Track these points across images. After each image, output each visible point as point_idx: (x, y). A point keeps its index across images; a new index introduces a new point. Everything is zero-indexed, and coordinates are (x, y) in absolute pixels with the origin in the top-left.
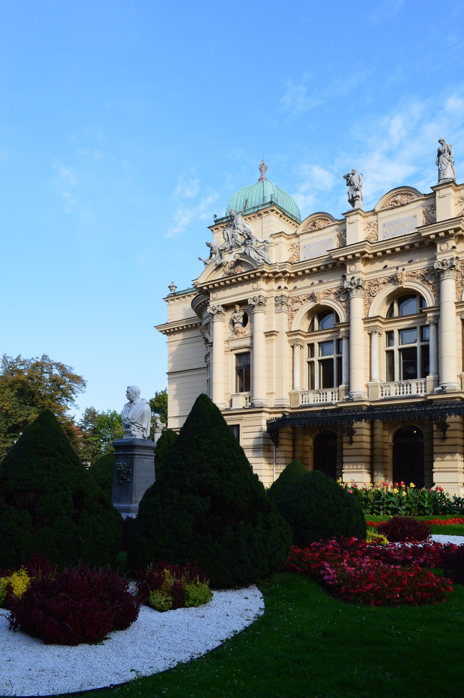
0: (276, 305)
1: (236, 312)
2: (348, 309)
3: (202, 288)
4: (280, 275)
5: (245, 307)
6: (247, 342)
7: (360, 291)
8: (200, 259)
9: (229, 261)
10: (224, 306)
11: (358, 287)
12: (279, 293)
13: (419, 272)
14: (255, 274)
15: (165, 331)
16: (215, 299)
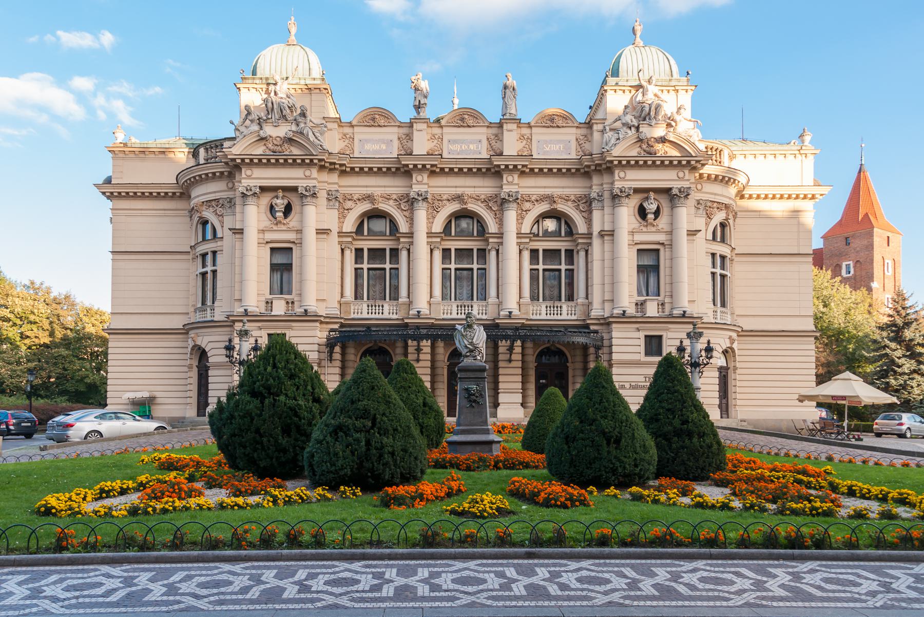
0: (329, 200)
1: (277, 197)
2: (411, 220)
3: (234, 160)
4: (337, 166)
5: (287, 194)
6: (291, 236)
7: (425, 204)
8: (232, 123)
9: (274, 135)
10: (260, 187)
11: (425, 199)
12: (335, 187)
13: (483, 197)
14: (311, 160)
15: (112, 193)
16: (249, 177)
